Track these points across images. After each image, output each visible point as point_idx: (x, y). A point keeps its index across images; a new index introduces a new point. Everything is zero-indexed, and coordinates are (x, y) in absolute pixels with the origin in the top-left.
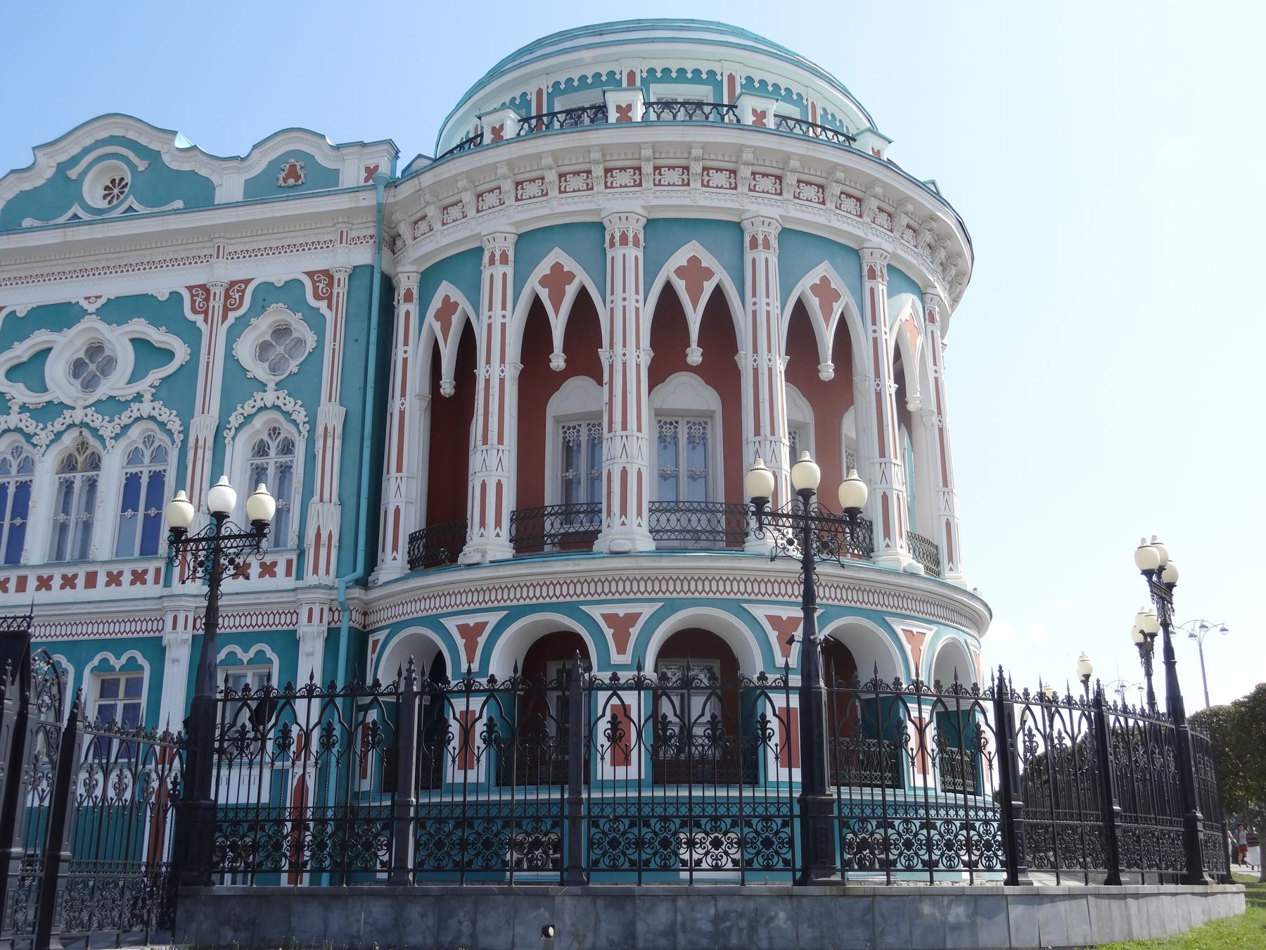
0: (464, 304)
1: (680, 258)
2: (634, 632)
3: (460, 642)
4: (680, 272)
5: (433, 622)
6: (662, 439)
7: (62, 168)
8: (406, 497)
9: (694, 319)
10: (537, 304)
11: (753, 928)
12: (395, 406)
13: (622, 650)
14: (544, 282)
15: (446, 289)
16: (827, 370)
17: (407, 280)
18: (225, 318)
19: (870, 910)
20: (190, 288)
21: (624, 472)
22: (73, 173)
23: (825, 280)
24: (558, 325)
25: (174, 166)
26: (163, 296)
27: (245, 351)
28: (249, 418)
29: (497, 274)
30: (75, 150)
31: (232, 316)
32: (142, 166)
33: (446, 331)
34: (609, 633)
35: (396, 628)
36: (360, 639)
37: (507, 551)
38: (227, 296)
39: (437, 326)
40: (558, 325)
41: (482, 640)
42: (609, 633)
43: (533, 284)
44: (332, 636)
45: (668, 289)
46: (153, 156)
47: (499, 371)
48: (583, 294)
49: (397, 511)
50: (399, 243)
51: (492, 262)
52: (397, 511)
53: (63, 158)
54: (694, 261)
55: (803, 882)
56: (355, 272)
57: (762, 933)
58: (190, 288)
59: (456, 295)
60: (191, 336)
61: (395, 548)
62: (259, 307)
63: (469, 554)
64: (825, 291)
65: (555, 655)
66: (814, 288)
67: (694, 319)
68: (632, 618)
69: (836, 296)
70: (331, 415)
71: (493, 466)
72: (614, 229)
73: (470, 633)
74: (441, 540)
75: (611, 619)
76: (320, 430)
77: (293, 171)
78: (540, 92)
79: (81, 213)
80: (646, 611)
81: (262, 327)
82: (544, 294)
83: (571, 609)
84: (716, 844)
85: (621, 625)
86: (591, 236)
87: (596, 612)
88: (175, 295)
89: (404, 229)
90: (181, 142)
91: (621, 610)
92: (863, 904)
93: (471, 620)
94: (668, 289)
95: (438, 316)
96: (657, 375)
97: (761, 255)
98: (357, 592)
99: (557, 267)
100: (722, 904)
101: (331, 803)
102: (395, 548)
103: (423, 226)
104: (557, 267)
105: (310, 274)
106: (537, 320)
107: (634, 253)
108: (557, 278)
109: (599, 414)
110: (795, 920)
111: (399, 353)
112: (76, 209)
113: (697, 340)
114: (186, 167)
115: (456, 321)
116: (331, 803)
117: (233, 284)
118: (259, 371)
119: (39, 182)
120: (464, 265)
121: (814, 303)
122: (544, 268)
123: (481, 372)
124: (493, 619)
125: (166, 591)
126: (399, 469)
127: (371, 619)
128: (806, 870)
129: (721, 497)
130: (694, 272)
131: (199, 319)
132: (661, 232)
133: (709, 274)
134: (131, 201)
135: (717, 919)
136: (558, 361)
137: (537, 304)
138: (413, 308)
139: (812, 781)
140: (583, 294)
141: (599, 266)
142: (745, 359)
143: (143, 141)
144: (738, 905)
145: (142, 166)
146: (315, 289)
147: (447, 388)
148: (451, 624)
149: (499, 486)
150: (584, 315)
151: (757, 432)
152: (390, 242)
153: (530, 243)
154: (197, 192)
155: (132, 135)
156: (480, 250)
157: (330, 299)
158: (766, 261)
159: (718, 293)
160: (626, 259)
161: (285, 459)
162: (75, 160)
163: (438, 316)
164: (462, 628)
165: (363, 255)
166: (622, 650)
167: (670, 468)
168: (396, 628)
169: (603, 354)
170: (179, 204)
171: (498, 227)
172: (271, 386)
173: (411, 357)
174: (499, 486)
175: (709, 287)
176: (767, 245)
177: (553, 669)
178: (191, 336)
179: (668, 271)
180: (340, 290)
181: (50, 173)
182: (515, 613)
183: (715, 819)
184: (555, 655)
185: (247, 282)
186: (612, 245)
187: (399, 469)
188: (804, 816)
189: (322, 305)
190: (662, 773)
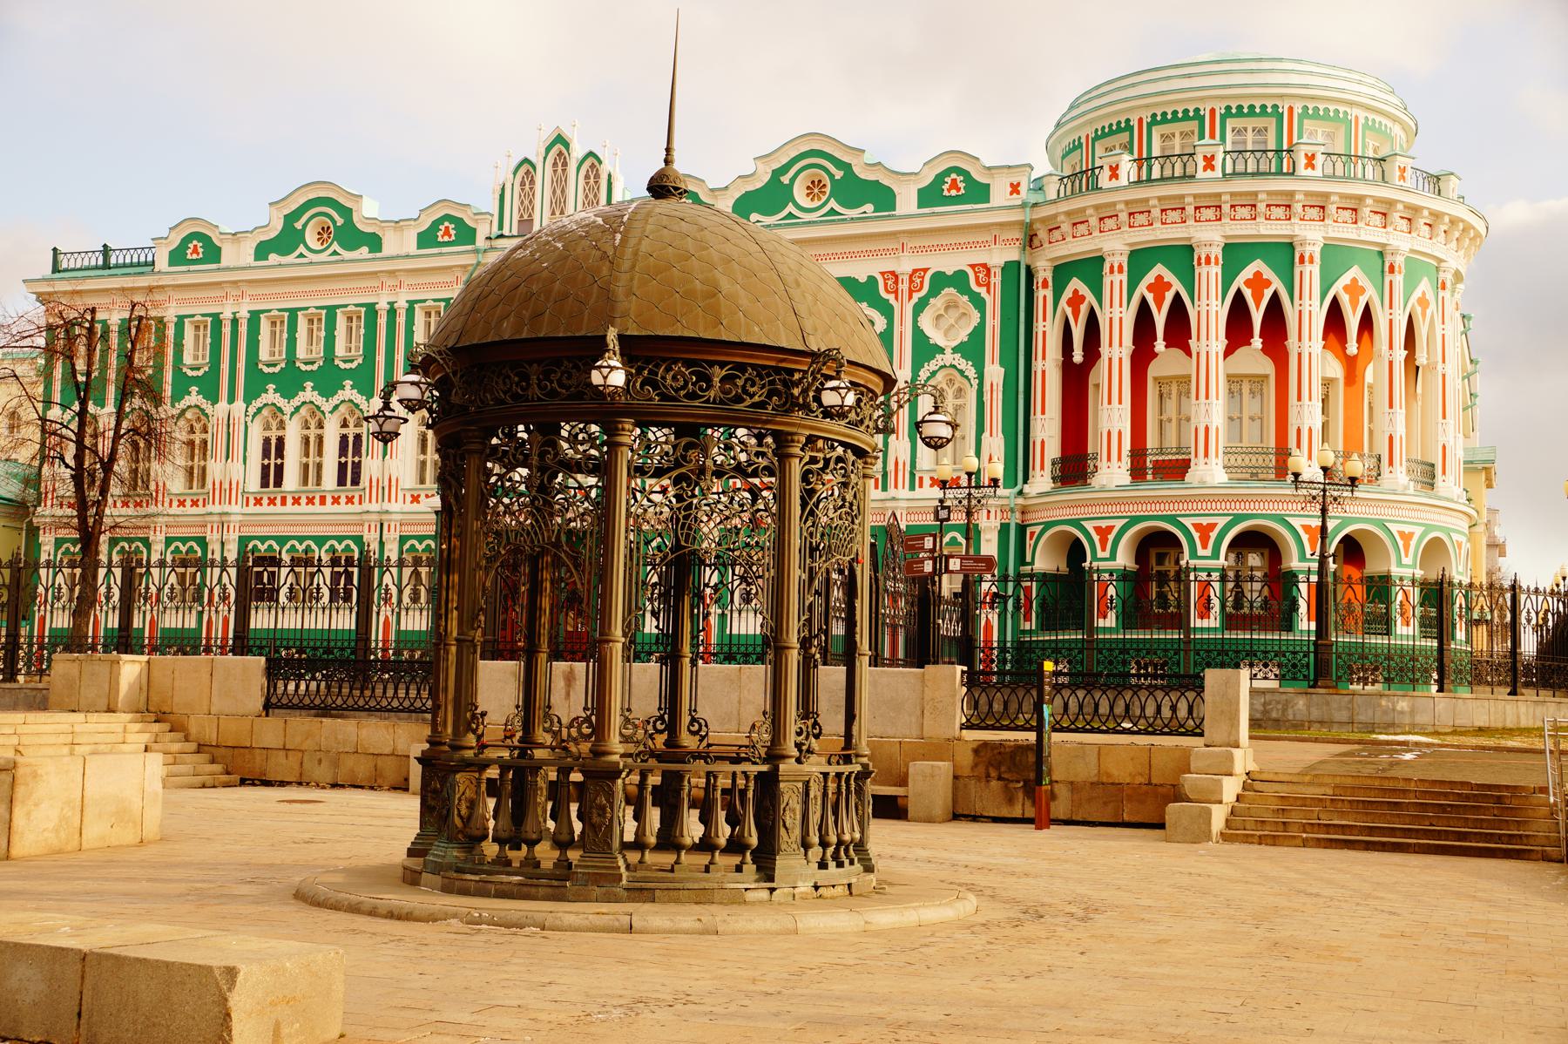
0: (1090, 298)
1: (1248, 273)
2: (1213, 535)
3: (1096, 538)
4: (1248, 283)
5: (1076, 523)
6: (1231, 392)
7: (777, 173)
8: (1048, 430)
9: (1257, 317)
10: (1144, 301)
11: (1284, 710)
12: (1038, 366)
13: (1205, 547)
14: (1150, 288)
15: (1076, 284)
16: (1352, 348)
17: (1044, 272)
18: (910, 298)
19: (1351, 701)
20: (882, 274)
21: (1207, 429)
22: (786, 179)
23: (1354, 280)
24: (1160, 320)
25: (862, 176)
26: (863, 279)
27: (926, 323)
28: (934, 374)
29: (1115, 281)
30: (785, 161)
31: (916, 296)
32: (838, 174)
33: (1076, 314)
34: (1196, 535)
35: (1048, 525)
36: (1022, 529)
37: (1127, 479)
38: (911, 281)
39: (1069, 311)
40: (1160, 320)
41: (1111, 537)
42: (1196, 535)
43: (1142, 289)
44: (1004, 529)
45: (1239, 293)
46: (846, 167)
47: (1117, 349)
48: (1177, 296)
49: (1043, 442)
50: (1036, 242)
51: (1112, 271)
52: (1043, 442)
53: (776, 166)
54: (1258, 274)
55: (1314, 687)
56: (1010, 268)
57: (1290, 711)
58: (882, 274)
59: (1084, 290)
60: (887, 311)
61: (1042, 468)
62: (935, 291)
63: (1097, 481)
64: (1354, 289)
65: (1157, 545)
66: (1346, 288)
67: (1257, 317)
68: (1212, 526)
69: (1363, 290)
70: (995, 373)
71: (1111, 417)
72: (1201, 252)
73: (1103, 533)
74: (1074, 466)
75: (1197, 527)
76: (987, 387)
77: (956, 185)
78: (1140, 120)
79: (796, 212)
80: (1221, 522)
81: (937, 303)
82: (1150, 297)
83: (1172, 519)
84: (1266, 666)
85: (1205, 531)
86: (1183, 257)
87: (1188, 522)
88: (872, 279)
89: (1042, 234)
90: (869, 158)
91: (1205, 521)
92: (1347, 698)
93: (1104, 524)
94: (1239, 293)
95: (1069, 302)
96: (1228, 352)
97: (1307, 268)
98: (1020, 501)
99: (1159, 278)
100: (1268, 697)
101: (1009, 638)
102: (1042, 468)
103: (1056, 234)
104: (1159, 278)
105: (973, 266)
106: (1144, 317)
107: (1215, 270)
108: (1159, 287)
109: (1189, 376)
110: (1308, 707)
111: (1039, 327)
112: (790, 208)
113: (1260, 326)
114: (873, 178)
115: (1084, 309)
116: (1009, 638)
117: (915, 271)
118: (936, 337)
119: (759, 185)
120: (1091, 268)
121: (1345, 301)
122: (1150, 278)
123: (1104, 349)
124: (1119, 524)
125: (883, 495)
126: (1043, 412)
127: (1028, 516)
128: (1316, 681)
129: (1272, 444)
130: (1258, 283)
131: (891, 298)
132: (1236, 254)
133: (1268, 283)
134: (833, 204)
135: (1264, 704)
136: (1160, 345)
137: (1144, 301)
138: (1049, 293)
139: (1322, 631)
140: (1177, 296)
141: (1189, 280)
142: (1292, 342)
143: (837, 154)
144: (1277, 697)
145: (838, 174)
146: (977, 278)
147: (1078, 357)
148: (1089, 526)
149: (1120, 433)
150: (1178, 312)
151: (1299, 399)
152: (1030, 240)
153: (1140, 259)
154: (883, 197)
155: (827, 150)
156: (1101, 259)
157: (988, 286)
158: (1311, 273)
159: (1275, 297)
160: (1210, 274)
161: (959, 402)
162: (784, 169)
163: (1069, 302)
164: (1097, 529)
165: (1013, 254)
166: (1205, 547)
167: (1236, 415)
168: (1048, 525)
169: (1192, 343)
170: (869, 208)
171: (1115, 246)
172: (948, 351)
173: (1048, 331)
174: (1120, 433)
175: (1268, 293)
176: (1311, 261)
177: (1153, 553)
178: (887, 311)
179: (1239, 282)
180: (996, 280)
181: (767, 178)
182: (1134, 520)
183: (1266, 652)
184: (1157, 545)
185: (925, 270)
186: (1199, 264)
187: (1043, 412)
188: (1316, 653)
189: (982, 291)
190: (1230, 622)
